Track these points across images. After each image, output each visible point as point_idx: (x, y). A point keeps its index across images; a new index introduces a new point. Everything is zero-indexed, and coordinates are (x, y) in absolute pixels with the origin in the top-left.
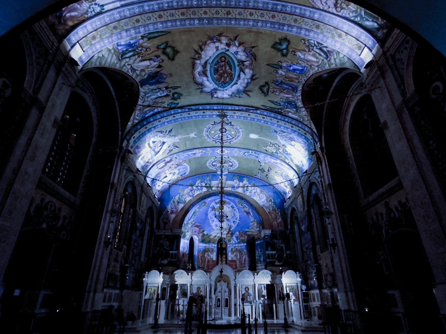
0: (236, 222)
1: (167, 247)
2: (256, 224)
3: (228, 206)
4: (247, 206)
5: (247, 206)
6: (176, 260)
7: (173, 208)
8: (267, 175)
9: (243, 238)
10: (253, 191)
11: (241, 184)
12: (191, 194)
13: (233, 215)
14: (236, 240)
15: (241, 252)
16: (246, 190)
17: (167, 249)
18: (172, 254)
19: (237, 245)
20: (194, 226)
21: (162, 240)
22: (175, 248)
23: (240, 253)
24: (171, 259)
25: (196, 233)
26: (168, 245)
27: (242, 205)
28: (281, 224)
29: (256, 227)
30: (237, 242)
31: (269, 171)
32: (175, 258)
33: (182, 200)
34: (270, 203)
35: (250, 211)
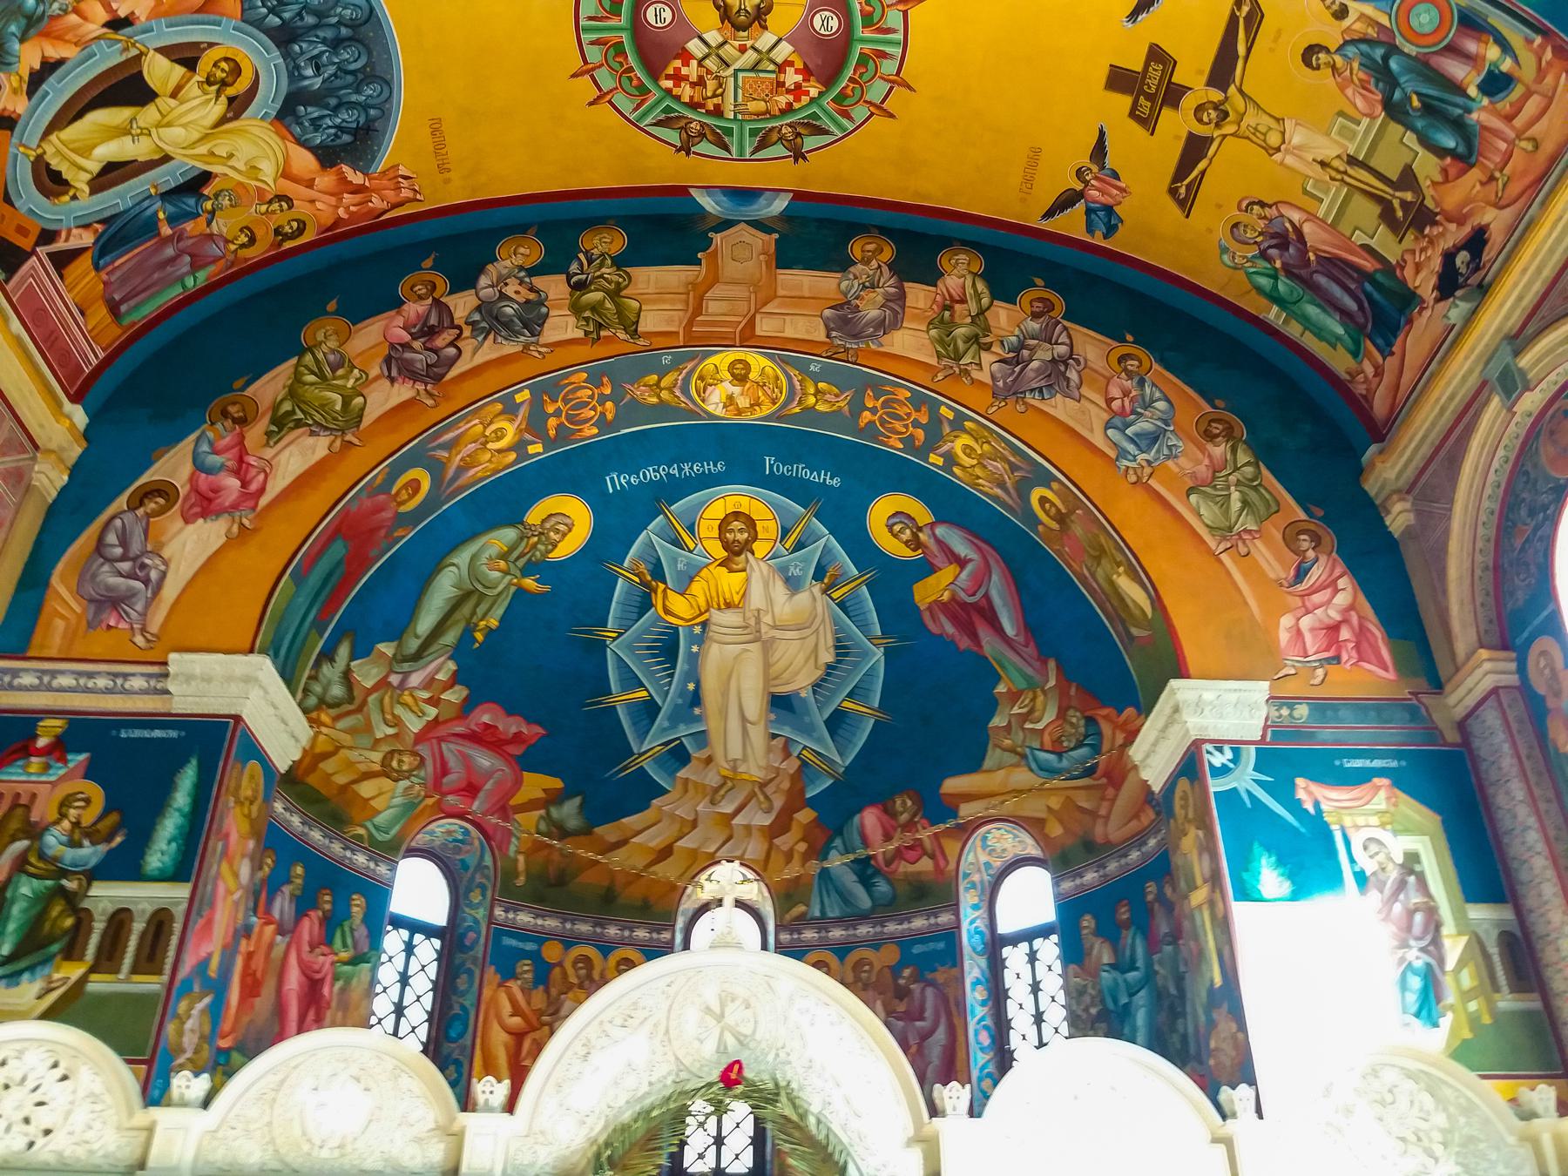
0: (861, 715)
1: (73, 844)
2: (1050, 715)
3: (783, 570)
4: (962, 548)
5: (962, 548)
6: (150, 984)
7: (209, 471)
8: (1195, 148)
9: (925, 864)
10: (1044, 354)
11: (918, 295)
12: (420, 358)
13: (828, 657)
14: (859, 891)
15: (902, 993)
16: (974, 339)
17: (70, 854)
18: (120, 920)
19: (864, 930)
20: (459, 729)
21: (36, 762)
22: (160, 853)
23: (901, 1007)
24: (93, 969)
25: (476, 805)
26: (88, 818)
27: (915, 543)
28: (1361, 633)
29: (1058, 741)
30: (865, 902)
31: (1222, 71)
32: (149, 960)
33: (325, 406)
34: (1219, 450)
35: (998, 590)
